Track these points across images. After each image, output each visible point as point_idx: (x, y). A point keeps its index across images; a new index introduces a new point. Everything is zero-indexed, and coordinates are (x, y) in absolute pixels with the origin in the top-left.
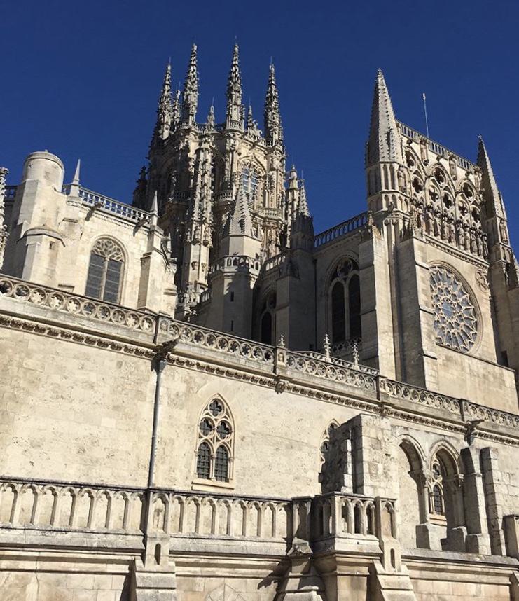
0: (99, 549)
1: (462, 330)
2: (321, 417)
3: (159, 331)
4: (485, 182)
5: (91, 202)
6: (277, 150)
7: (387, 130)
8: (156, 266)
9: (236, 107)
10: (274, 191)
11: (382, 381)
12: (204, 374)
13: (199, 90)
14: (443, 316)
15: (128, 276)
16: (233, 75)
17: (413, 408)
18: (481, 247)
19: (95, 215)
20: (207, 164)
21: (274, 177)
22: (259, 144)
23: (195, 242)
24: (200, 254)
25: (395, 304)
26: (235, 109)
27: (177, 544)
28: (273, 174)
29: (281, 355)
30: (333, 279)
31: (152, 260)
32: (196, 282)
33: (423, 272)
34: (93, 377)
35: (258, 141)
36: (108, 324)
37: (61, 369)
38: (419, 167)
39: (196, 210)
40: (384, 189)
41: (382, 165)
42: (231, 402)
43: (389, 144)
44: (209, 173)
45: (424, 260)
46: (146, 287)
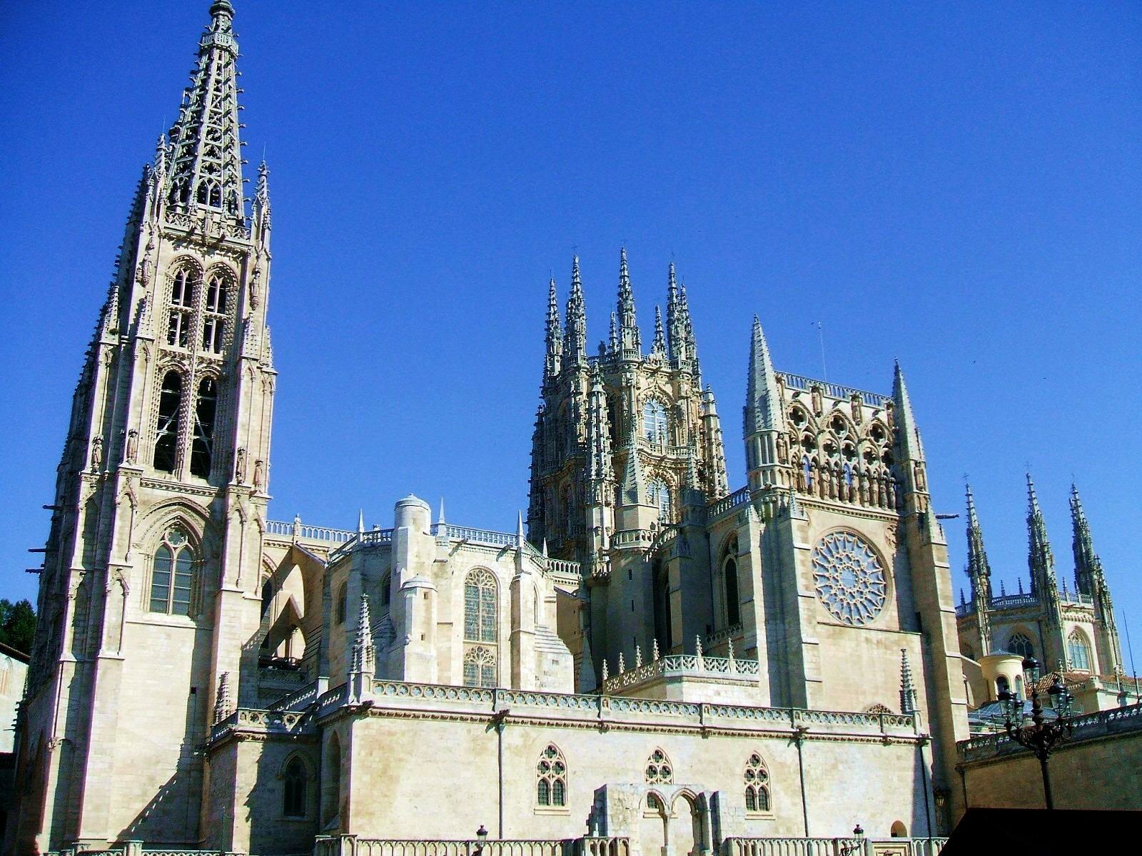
1: (866, 598)
4: (898, 419)
7: (764, 393)
10: (685, 424)
12: (537, 728)
14: (843, 587)
15: (502, 601)
19: (463, 548)
20: (601, 410)
21: (684, 407)
22: (661, 369)
23: (597, 504)
26: (628, 334)
28: (682, 404)
29: (605, 702)
35: (660, 368)
36: (456, 703)
39: (594, 467)
40: (761, 465)
42: (561, 746)
44: (605, 420)
45: (805, 540)
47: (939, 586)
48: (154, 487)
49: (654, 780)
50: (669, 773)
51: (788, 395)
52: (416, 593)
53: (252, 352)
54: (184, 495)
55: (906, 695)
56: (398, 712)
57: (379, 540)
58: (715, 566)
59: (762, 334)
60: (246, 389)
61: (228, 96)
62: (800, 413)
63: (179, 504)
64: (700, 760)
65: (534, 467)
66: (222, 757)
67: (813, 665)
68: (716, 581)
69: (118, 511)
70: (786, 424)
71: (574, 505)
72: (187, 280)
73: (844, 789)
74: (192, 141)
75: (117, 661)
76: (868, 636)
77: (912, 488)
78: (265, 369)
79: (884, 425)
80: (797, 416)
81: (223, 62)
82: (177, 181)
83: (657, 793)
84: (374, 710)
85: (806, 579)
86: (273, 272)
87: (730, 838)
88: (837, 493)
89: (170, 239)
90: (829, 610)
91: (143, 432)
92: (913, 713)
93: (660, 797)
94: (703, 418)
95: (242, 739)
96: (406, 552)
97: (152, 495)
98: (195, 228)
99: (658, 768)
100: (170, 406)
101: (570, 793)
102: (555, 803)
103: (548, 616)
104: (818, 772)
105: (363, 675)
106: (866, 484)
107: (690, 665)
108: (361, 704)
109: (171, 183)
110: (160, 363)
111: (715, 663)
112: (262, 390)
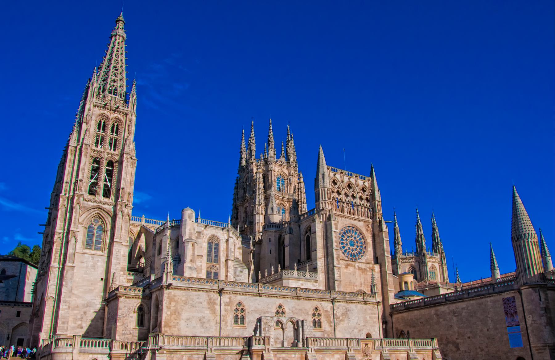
0: (198, 349)
1: (358, 251)
2: (275, 303)
3: (220, 285)
5: (206, 223)
7: (323, 173)
8: (231, 243)
9: (272, 150)
10: (292, 186)
13: (256, 142)
16: (270, 134)
17: (311, 296)
18: (369, 214)
20: (261, 179)
21: (291, 179)
23: (257, 214)
24: (260, 219)
25: (325, 247)
27: (216, 348)
30: (306, 234)
31: (229, 241)
32: (259, 231)
33: (336, 234)
34: (201, 300)
37: (192, 300)
38: (339, 185)
40: (321, 199)
41: (320, 189)
42: (244, 303)
43: (323, 179)
44: (262, 182)
45: (336, 228)
46: (228, 252)
47: (385, 247)
49: (278, 316)
50: (284, 313)
51: (332, 174)
52: (189, 244)
53: (128, 151)
54: (100, 205)
55: (372, 287)
56: (181, 288)
58: (302, 237)
59: (322, 151)
60: (125, 165)
61: (122, 54)
62: (336, 182)
63: (98, 208)
64: (296, 309)
65: (234, 199)
66: (112, 304)
67: (338, 275)
68: (302, 243)
69: (74, 210)
70: (330, 185)
71: (249, 214)
73: (349, 321)
74: (107, 70)
75: (73, 267)
77: (376, 211)
78: (133, 158)
80: (334, 182)
81: (120, 41)
82: (101, 85)
84: (173, 287)
85: (336, 243)
86: (137, 121)
87: (308, 337)
89: (98, 107)
90: (344, 255)
91: (84, 180)
92: (375, 293)
94: (298, 183)
95: (120, 297)
96: (185, 228)
97: (87, 204)
98: (107, 103)
99: (280, 311)
100: (96, 170)
101: (246, 320)
102: (241, 323)
103: (238, 254)
104: (340, 314)
105: (168, 273)
106: (360, 209)
107: (292, 274)
108: (167, 284)
109: (99, 86)
110: (92, 154)
111: (302, 273)
112: (131, 166)
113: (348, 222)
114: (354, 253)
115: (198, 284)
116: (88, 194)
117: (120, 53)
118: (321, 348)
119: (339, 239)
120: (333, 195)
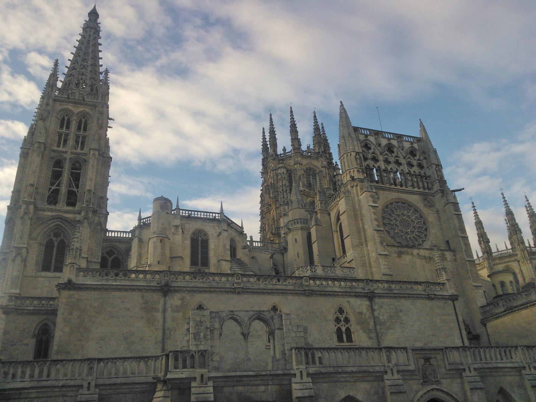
1: (416, 235)
6: (323, 156)
11: (306, 279)
14: (401, 229)
27: (100, 382)
30: (338, 222)
48: (44, 210)
54: (60, 214)
57: (149, 222)
58: (334, 228)
62: (369, 146)
63: (57, 218)
72: (68, 119)
76: (419, 252)
79: (416, 149)
80: (367, 146)
81: (92, 33)
83: (237, 317)
88: (392, 182)
90: (395, 240)
93: (239, 320)
100: (57, 176)
104: (386, 318)
113: (394, 195)
114: (410, 238)
115: (124, 280)
116: (46, 204)
117: (91, 45)
118: (323, 370)
119: (383, 218)
120: (368, 162)
